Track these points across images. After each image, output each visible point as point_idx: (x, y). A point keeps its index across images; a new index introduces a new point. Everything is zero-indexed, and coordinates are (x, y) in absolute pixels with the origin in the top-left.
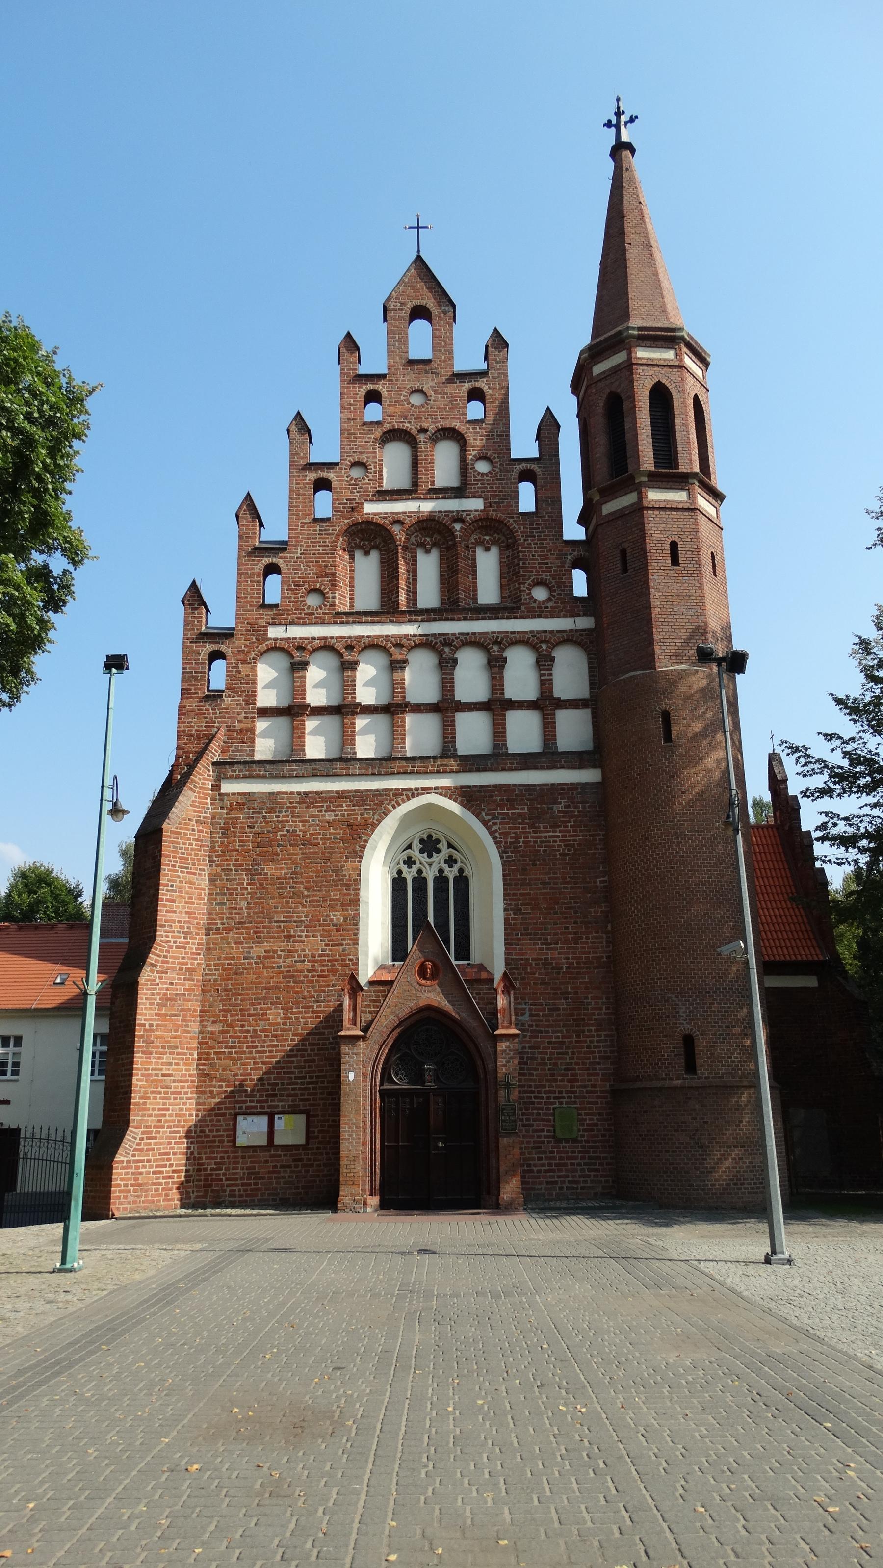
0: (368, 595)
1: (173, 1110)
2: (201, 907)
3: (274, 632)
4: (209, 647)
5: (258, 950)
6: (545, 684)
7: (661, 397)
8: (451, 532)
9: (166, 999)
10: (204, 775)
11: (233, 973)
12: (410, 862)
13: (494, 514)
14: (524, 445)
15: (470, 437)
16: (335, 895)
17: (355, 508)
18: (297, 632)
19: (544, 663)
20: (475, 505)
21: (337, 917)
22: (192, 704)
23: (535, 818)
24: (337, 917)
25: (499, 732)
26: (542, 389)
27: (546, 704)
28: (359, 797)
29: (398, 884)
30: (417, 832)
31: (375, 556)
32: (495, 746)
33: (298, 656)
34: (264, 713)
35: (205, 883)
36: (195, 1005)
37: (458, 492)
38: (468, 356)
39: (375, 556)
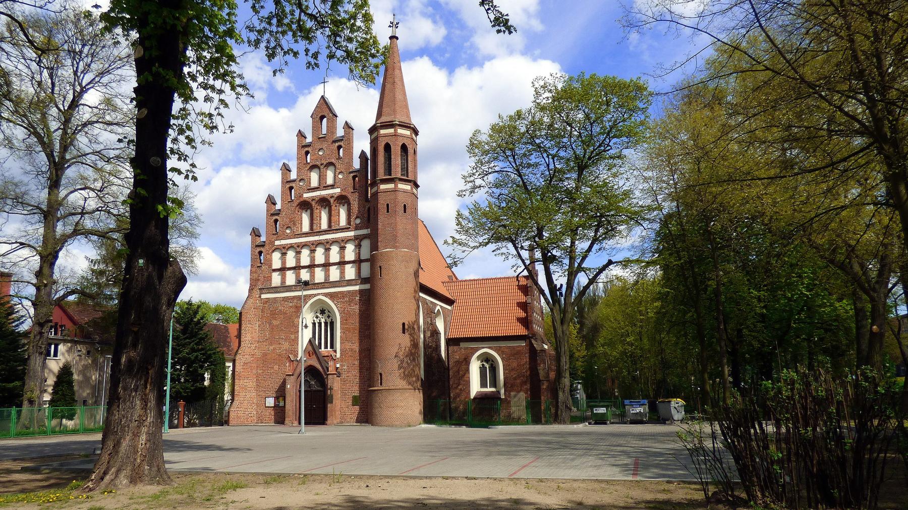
0: (306, 228)
1: (248, 396)
2: (256, 335)
3: (277, 243)
4: (259, 249)
5: (271, 348)
6: (359, 254)
7: (388, 148)
8: (329, 202)
9: (245, 364)
10: (256, 293)
11: (265, 355)
12: (317, 317)
13: (344, 194)
14: (357, 164)
15: (337, 165)
16: (292, 330)
17: (301, 196)
18: (283, 242)
19: (359, 246)
20: (337, 191)
21: (293, 337)
22: (254, 269)
23: (350, 302)
24: (293, 337)
25: (342, 273)
26: (362, 144)
27: (358, 262)
28: (299, 298)
29: (314, 324)
30: (318, 307)
31: (309, 211)
32: (341, 278)
33: (284, 251)
34: (274, 270)
35: (257, 328)
36: (254, 365)
37: (332, 186)
38: (340, 132)
39: (309, 211)
